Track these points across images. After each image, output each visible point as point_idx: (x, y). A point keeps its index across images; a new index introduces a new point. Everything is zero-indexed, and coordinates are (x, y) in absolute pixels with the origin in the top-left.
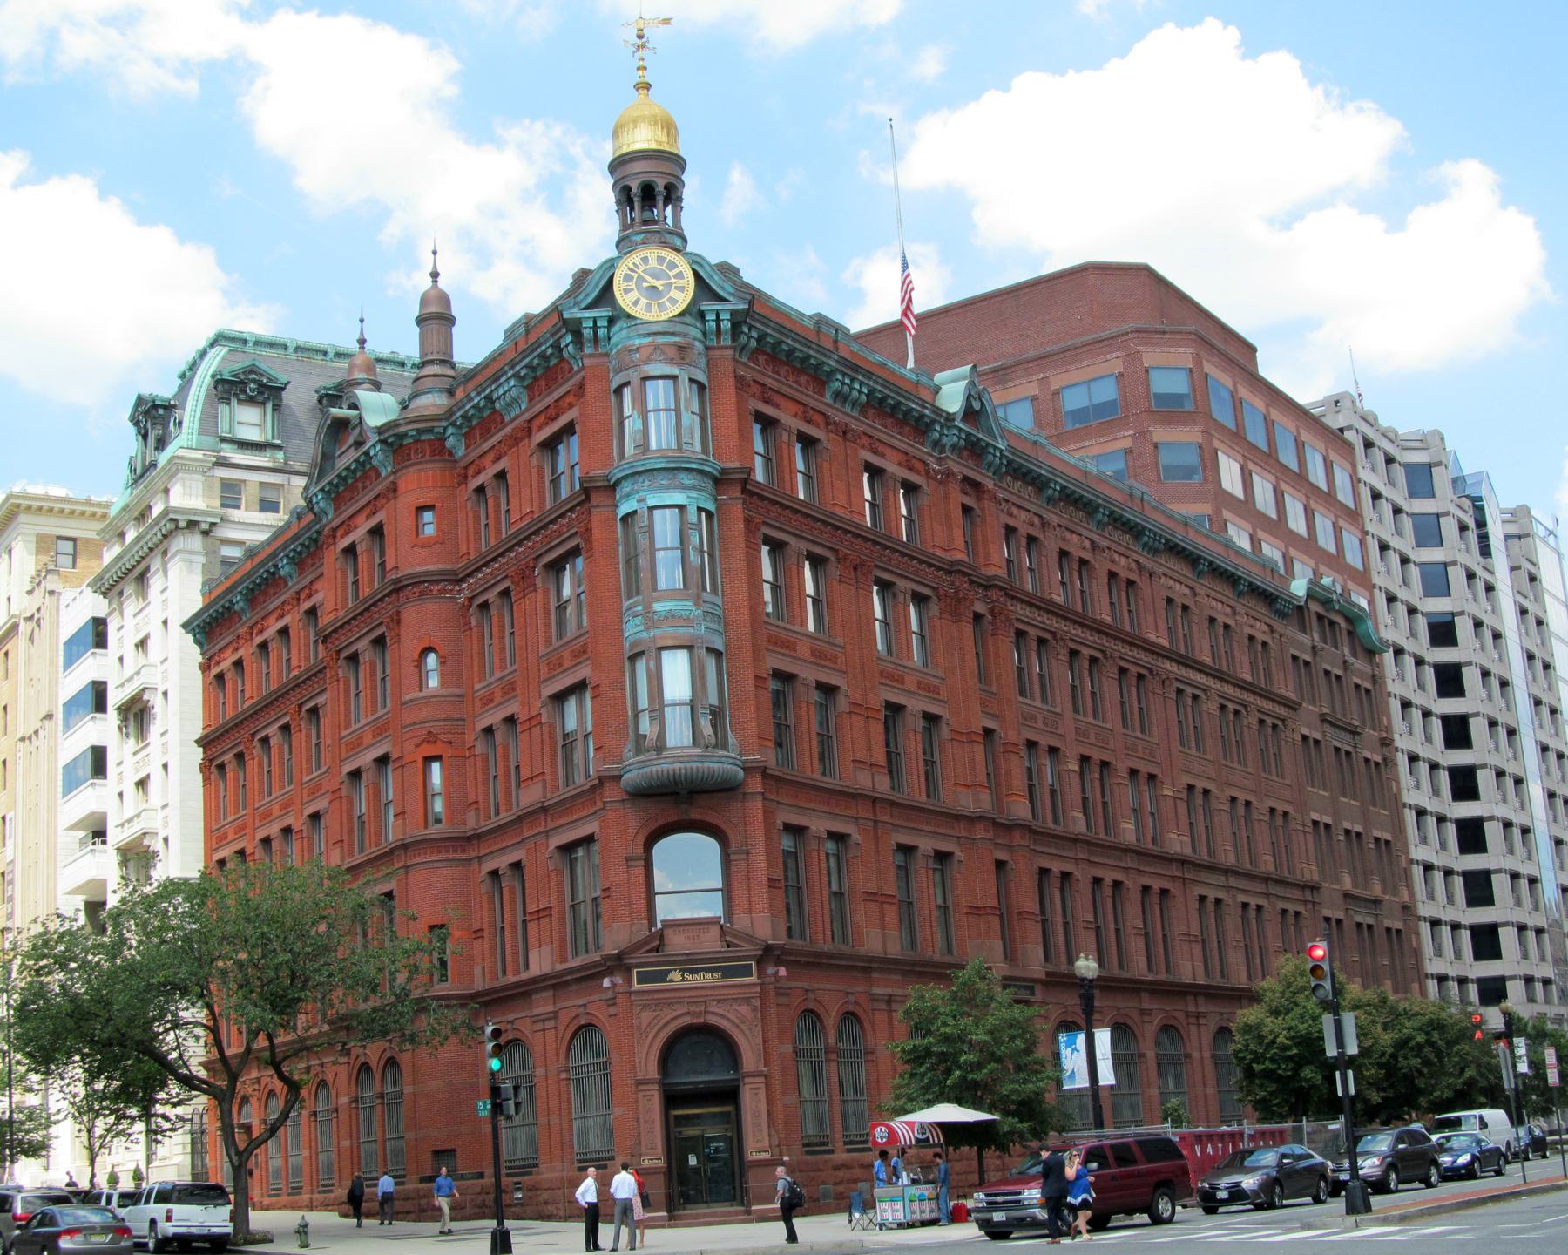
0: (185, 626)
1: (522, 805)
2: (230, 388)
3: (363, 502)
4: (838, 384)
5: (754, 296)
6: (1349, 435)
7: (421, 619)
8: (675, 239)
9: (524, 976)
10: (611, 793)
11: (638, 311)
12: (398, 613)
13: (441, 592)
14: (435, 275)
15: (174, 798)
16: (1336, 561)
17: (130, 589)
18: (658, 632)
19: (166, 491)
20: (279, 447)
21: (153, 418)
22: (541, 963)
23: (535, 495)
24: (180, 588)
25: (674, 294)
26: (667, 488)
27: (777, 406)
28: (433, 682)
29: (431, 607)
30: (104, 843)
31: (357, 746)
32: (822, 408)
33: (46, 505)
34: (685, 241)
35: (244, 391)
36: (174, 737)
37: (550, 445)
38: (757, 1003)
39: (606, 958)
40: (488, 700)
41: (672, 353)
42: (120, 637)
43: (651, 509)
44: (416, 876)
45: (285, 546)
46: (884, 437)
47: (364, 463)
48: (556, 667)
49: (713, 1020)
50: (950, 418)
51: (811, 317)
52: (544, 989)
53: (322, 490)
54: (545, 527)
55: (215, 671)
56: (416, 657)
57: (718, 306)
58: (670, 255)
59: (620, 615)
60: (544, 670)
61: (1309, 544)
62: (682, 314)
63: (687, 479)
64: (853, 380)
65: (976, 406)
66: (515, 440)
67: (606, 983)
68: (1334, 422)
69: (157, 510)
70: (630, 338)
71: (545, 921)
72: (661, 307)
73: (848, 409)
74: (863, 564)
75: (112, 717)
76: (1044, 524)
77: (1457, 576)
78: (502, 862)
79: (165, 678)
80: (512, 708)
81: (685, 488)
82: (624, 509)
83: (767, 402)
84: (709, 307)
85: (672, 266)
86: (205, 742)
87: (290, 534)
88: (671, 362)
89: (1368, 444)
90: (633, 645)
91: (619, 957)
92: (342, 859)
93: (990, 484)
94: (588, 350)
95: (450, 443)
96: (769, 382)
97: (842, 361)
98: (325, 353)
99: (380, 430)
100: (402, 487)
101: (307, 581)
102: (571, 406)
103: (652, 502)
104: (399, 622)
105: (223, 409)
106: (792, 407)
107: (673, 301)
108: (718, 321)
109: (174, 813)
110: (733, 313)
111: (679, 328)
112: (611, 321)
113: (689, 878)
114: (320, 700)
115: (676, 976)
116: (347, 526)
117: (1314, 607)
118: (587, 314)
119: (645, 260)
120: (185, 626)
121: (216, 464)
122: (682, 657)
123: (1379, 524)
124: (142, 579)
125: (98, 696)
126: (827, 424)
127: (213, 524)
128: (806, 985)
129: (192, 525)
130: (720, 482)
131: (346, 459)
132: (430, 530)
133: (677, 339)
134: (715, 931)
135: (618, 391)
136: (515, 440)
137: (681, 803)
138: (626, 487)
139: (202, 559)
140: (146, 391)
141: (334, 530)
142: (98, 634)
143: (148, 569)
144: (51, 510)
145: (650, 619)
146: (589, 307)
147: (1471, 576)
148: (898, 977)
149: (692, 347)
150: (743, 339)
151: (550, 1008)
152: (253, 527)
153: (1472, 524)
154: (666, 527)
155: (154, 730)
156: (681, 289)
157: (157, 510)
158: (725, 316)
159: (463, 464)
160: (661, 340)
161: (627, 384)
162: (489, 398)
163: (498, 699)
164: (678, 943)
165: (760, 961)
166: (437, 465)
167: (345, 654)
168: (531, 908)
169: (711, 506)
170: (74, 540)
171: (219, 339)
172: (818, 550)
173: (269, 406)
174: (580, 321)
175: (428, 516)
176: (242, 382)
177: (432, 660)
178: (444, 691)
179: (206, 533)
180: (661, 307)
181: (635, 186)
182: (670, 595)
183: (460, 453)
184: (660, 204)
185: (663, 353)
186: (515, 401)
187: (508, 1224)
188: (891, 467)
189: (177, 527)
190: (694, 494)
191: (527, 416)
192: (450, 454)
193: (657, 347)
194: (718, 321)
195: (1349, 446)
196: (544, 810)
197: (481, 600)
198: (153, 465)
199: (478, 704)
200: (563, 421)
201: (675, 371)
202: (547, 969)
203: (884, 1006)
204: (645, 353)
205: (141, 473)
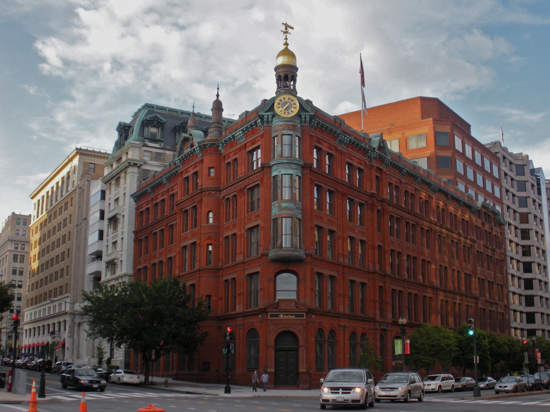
0: (131, 196)
3: (192, 164)
4: (340, 138)
5: (317, 110)
6: (498, 155)
8: (293, 92)
11: (282, 115)
12: (201, 199)
14: (218, 95)
15: (125, 248)
16: (492, 196)
17: (113, 182)
18: (282, 212)
19: (127, 153)
20: (162, 141)
21: (124, 130)
22: (239, 309)
23: (246, 167)
24: (130, 184)
25: (292, 109)
27: (321, 144)
28: (211, 221)
30: (101, 260)
31: (186, 238)
32: (334, 145)
34: (297, 93)
35: (153, 123)
36: (126, 230)
37: (251, 152)
38: (305, 325)
39: (260, 309)
40: (228, 228)
42: (110, 196)
43: (282, 175)
45: (165, 174)
46: (353, 154)
47: (193, 152)
49: (292, 330)
50: (374, 149)
51: (333, 117)
52: (241, 317)
53: (179, 159)
55: (141, 210)
56: (206, 213)
58: (292, 97)
61: (483, 190)
62: (295, 116)
63: (294, 166)
64: (345, 137)
65: (382, 145)
67: (260, 316)
68: (494, 151)
69: (124, 159)
71: (242, 296)
73: (343, 145)
74: (345, 193)
75: (106, 222)
76: (401, 182)
78: (229, 277)
79: (124, 211)
80: (235, 231)
82: (274, 174)
83: (319, 143)
84: (303, 114)
85: (292, 101)
86: (136, 233)
88: (291, 130)
89: (504, 158)
90: (274, 216)
91: (264, 309)
92: (179, 273)
93: (385, 170)
94: (265, 124)
95: (220, 148)
96: (319, 137)
97: (342, 131)
98: (178, 112)
99: (199, 143)
101: (172, 185)
102: (259, 141)
104: (201, 202)
105: (146, 129)
106: (327, 145)
107: (292, 112)
108: (305, 118)
109: (125, 254)
110: (310, 116)
111: (294, 120)
112: (273, 116)
113: (287, 286)
114: (174, 222)
115: (282, 316)
116: (187, 171)
118: (266, 114)
119: (284, 98)
120: (131, 196)
122: (289, 220)
123: (506, 184)
124: (118, 179)
126: (336, 150)
127: (141, 165)
128: (320, 321)
129: (135, 164)
130: (303, 167)
131: (187, 151)
134: (294, 303)
135: (274, 138)
136: (240, 149)
137: (287, 264)
138: (275, 167)
141: (182, 172)
143: (119, 177)
146: (266, 112)
147: (534, 201)
148: (348, 320)
150: (313, 124)
151: (242, 323)
153: (535, 184)
154: (286, 181)
155: (120, 226)
156: (295, 108)
158: (308, 117)
159: (224, 155)
160: (288, 123)
161: (277, 136)
162: (233, 136)
163: (231, 228)
164: (283, 306)
165: (307, 313)
167: (183, 210)
168: (238, 292)
169: (300, 175)
170: (94, 164)
172: (331, 189)
173: (160, 129)
174: (263, 116)
175: (212, 170)
176: (152, 120)
177: (211, 215)
178: (214, 224)
179: (139, 167)
180: (289, 113)
181: (282, 75)
182: (286, 201)
183: (223, 151)
184: (289, 80)
186: (241, 137)
187: (230, 386)
188: (355, 164)
190: (295, 171)
191: (245, 143)
192: (220, 152)
194: (305, 118)
195: (498, 159)
197: (227, 197)
201: (292, 133)
202: (242, 311)
203: (342, 328)
205: (119, 145)
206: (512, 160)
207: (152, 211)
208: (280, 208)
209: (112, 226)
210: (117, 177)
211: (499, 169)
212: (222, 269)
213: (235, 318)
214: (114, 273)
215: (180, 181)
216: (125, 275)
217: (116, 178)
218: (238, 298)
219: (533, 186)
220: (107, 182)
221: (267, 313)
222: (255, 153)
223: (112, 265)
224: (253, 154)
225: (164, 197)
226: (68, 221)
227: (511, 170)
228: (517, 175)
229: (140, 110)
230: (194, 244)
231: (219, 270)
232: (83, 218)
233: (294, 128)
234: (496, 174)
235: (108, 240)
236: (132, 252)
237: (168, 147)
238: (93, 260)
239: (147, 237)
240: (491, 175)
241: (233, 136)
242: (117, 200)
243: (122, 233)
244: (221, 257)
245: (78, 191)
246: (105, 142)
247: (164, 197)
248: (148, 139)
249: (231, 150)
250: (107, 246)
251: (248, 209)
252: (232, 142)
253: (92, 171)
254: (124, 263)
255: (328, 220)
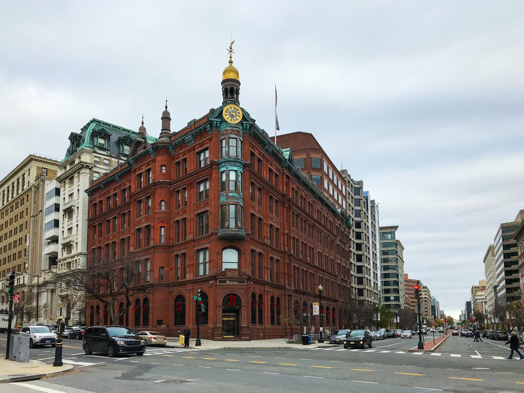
1: (187, 239)
2: (95, 134)
3: (145, 163)
7: (160, 193)
9: (184, 280)
10: (213, 237)
13: (166, 187)
15: (80, 232)
17: (67, 181)
19: (80, 157)
20: (109, 150)
24: (83, 181)
26: (233, 166)
28: (163, 208)
29: (163, 190)
31: (140, 222)
33: (40, 159)
36: (80, 218)
37: (199, 153)
40: (178, 214)
41: (236, 132)
42: (65, 191)
44: (156, 255)
48: (199, 207)
49: (236, 293)
52: (191, 283)
54: (198, 173)
59: (219, 196)
60: (195, 207)
66: (189, 151)
67: (211, 282)
69: (77, 161)
72: (234, 120)
75: (61, 212)
77: (362, 213)
78: (180, 253)
81: (237, 166)
82: (222, 170)
87: (117, 171)
88: (236, 134)
91: (215, 276)
98: (120, 129)
100: (157, 160)
101: (124, 182)
102: (207, 143)
103: (229, 169)
105: (95, 139)
108: (246, 126)
113: (230, 259)
117: (340, 216)
121: (93, 152)
124: (72, 179)
125: (57, 208)
130: (245, 166)
131: (141, 151)
132: (164, 171)
135: (222, 141)
136: (189, 151)
137: (231, 241)
139: (89, 175)
140: (74, 132)
142: (57, 192)
144: (41, 160)
145: (228, 197)
151: (192, 288)
152: (102, 170)
155: (74, 216)
157: (77, 161)
159: (173, 156)
160: (234, 128)
161: (225, 139)
162: (183, 140)
163: (181, 213)
164: (229, 274)
165: (247, 280)
167: (137, 200)
168: (188, 263)
171: (94, 121)
175: (164, 168)
177: (163, 203)
179: (90, 169)
186: (191, 141)
189: (83, 167)
193: (233, 130)
194: (246, 126)
196: (194, 241)
198: (76, 151)
199: (175, 215)
200: (205, 147)
201: (236, 137)
202: (191, 278)
204: (230, 131)
206: (352, 183)
207: (105, 203)
208: (228, 197)
209: (67, 216)
210: (71, 177)
211: (346, 189)
212: (173, 246)
213: (185, 284)
214: (70, 253)
215: (133, 177)
216: (81, 254)
217: (69, 178)
218: (188, 269)
219: (364, 203)
220: (61, 180)
221: (216, 279)
222: (202, 154)
223: (68, 246)
224: (200, 155)
225: (117, 191)
226: (25, 213)
227: (351, 191)
228: (355, 195)
229: (89, 124)
230: (148, 227)
231: (170, 247)
232: (40, 210)
233: (238, 133)
234: (344, 193)
235: (63, 227)
236: (86, 236)
237: (113, 155)
238: (49, 243)
239: (100, 224)
240: (341, 192)
241: (183, 140)
242: (71, 195)
243: (77, 221)
244: (172, 237)
245: (33, 189)
246: (58, 151)
247: (117, 191)
248: (97, 147)
249: (181, 152)
250: (63, 232)
251: (197, 199)
252: (182, 144)
253: (45, 174)
254: (79, 245)
255: (258, 210)
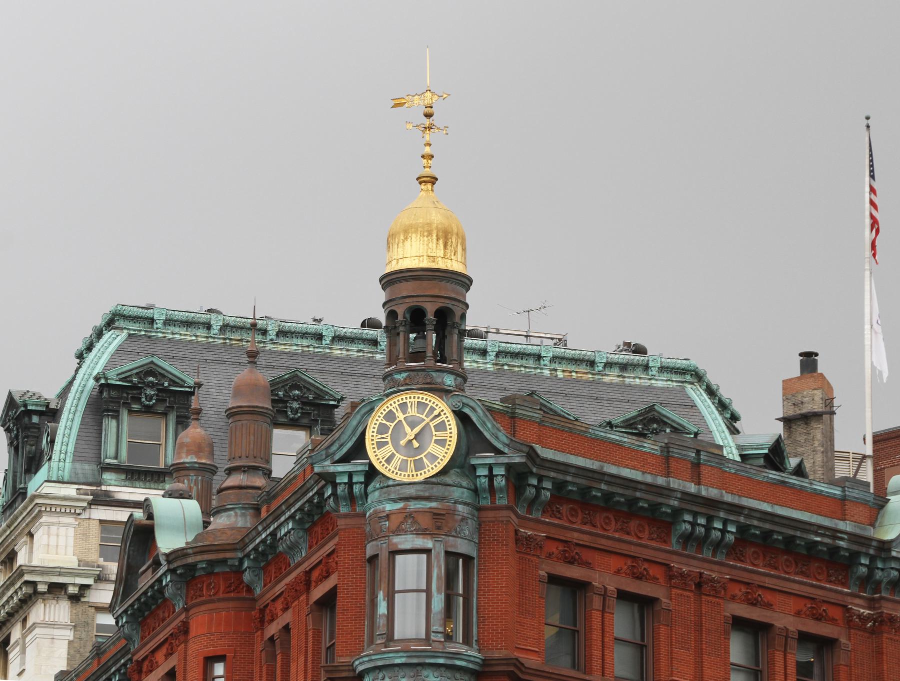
41: (425, 521)
57: (490, 458)
62: (444, 472)
70: (380, 502)
88: (423, 532)
95: (247, 577)
108: (491, 477)
110: (509, 467)
118: (340, 468)
119: (403, 407)
133: (434, 504)
146: (345, 460)
149: (452, 513)
150: (530, 492)
156: (441, 443)
158: (499, 471)
166: (231, 604)
174: (334, 475)
185: (415, 522)
194: (491, 477)
